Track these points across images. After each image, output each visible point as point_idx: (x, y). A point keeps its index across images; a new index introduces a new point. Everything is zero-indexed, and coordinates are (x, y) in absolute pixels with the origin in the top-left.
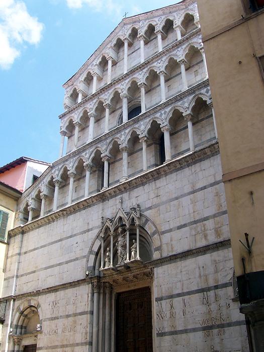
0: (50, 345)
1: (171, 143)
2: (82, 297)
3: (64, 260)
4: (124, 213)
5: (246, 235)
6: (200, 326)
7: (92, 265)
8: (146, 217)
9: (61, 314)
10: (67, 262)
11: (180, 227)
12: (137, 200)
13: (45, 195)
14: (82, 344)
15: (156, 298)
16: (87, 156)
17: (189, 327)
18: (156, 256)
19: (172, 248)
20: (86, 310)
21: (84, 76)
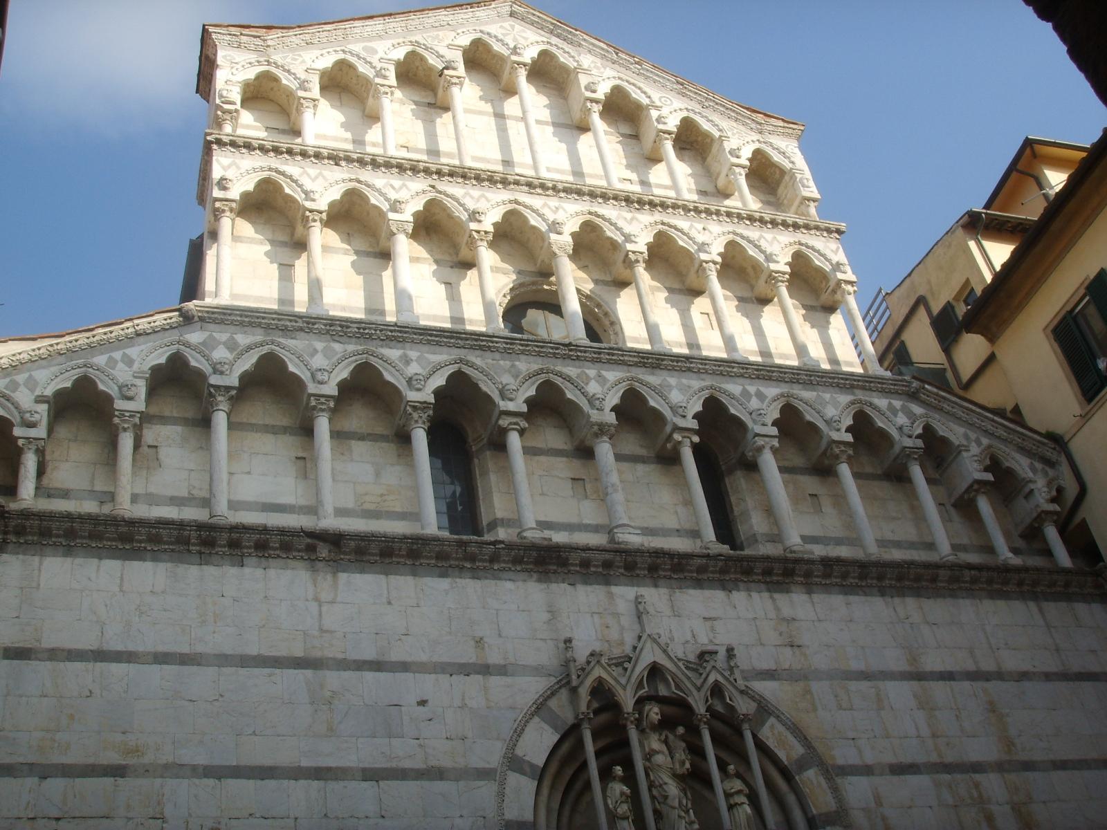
10: (372, 775)
11: (900, 769)
12: (713, 629)
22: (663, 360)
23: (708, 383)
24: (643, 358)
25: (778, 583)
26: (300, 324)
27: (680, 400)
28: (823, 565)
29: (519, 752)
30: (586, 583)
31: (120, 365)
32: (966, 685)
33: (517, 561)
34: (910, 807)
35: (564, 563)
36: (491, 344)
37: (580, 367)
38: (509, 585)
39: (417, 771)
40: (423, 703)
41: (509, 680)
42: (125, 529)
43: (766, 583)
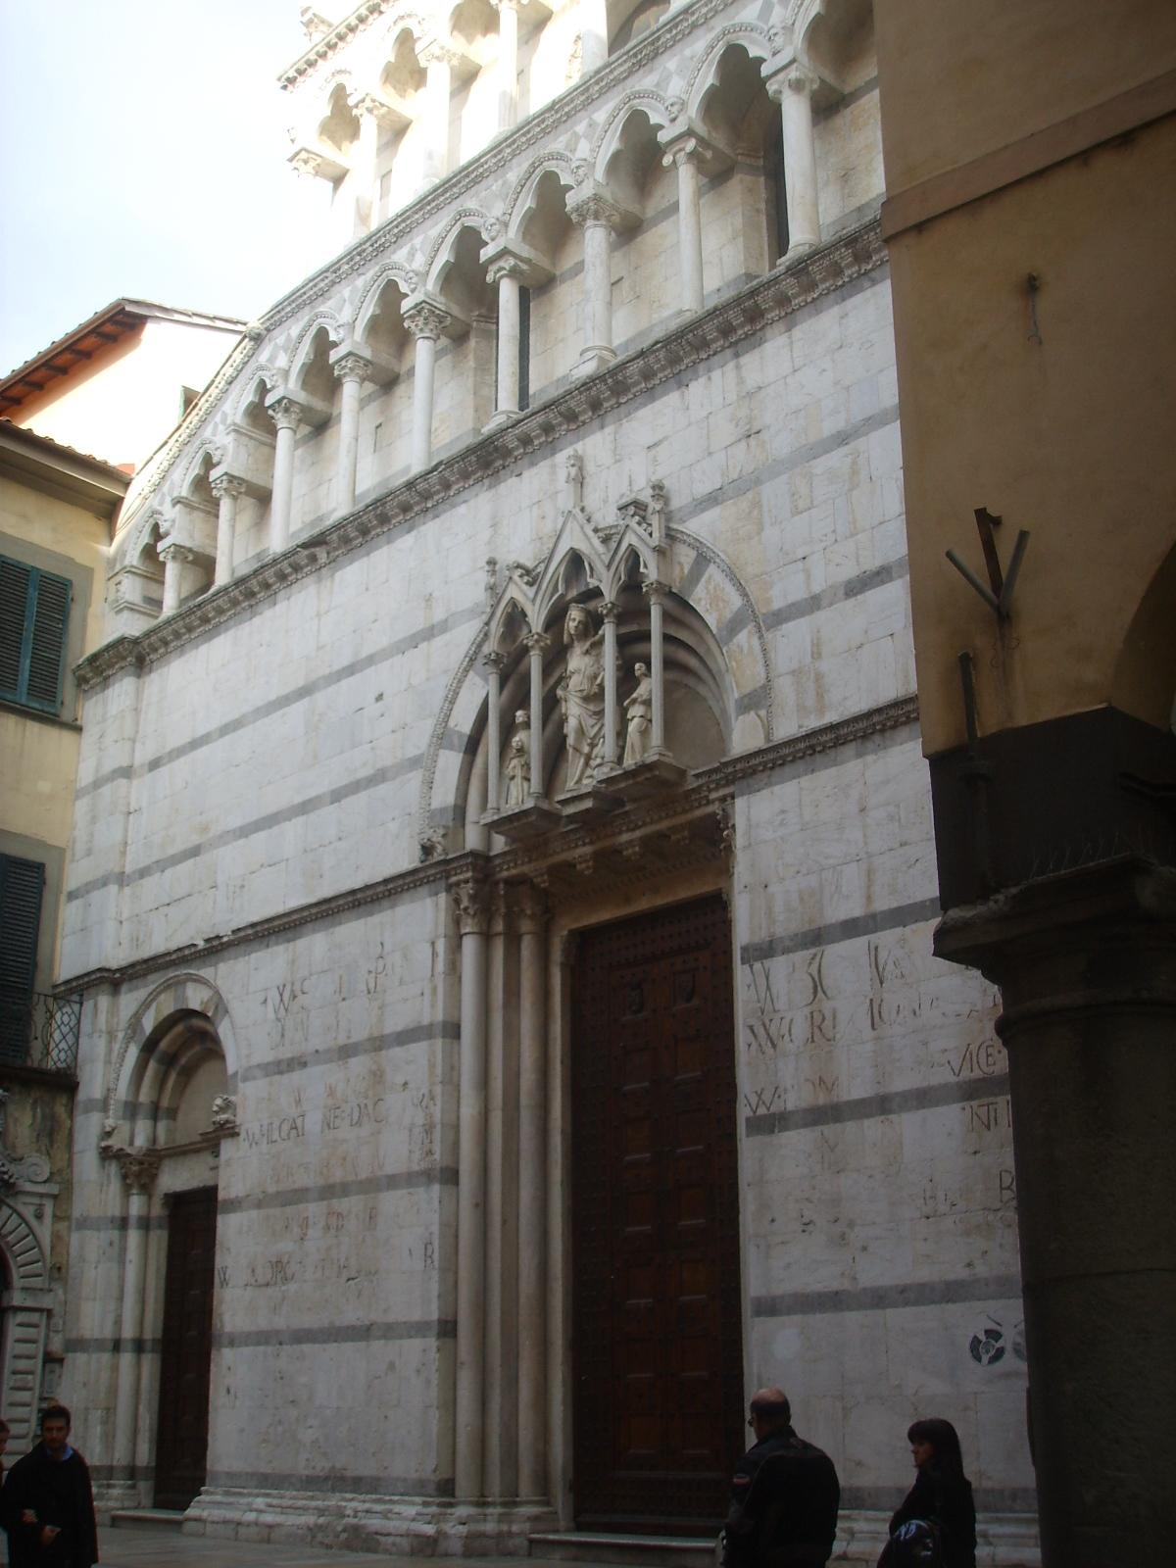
0: (272, 1189)
1: (816, 161)
2: (405, 956)
3: (323, 786)
4: (589, 529)
5: (987, 522)
6: (952, 1079)
8: (697, 545)
9: (317, 1042)
10: (337, 796)
12: (655, 460)
13: (232, 478)
14: (410, 1179)
15: (744, 949)
16: (419, 262)
17: (900, 1084)
18: (744, 737)
19: (820, 696)
20: (426, 1021)
22: (659, 38)
23: (718, 30)
24: (635, 55)
25: (747, 336)
26: (332, 276)
28: (792, 275)
30: (533, 464)
33: (465, 476)
34: (861, 646)
35: (506, 453)
36: (481, 170)
37: (567, 131)
38: (462, 509)
41: (446, 637)
42: (199, 613)
43: (732, 345)
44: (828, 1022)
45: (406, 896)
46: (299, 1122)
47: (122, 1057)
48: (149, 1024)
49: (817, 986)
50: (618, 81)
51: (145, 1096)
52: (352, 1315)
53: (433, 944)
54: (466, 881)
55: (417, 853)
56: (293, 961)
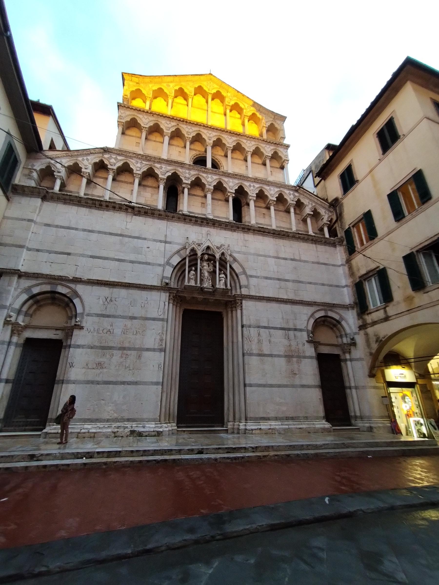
7: (170, 276)
9: (120, 313)
10: (132, 262)
21: (156, 87)
27: (231, 186)
29: (170, 261)
31: (85, 160)
32: (290, 262)
38: (176, 224)
39: (143, 262)
40: (148, 248)
44: (261, 341)
45: (157, 291)
46: (111, 331)
47: (18, 297)
48: (36, 290)
49: (259, 335)
50: (219, 174)
51: (25, 309)
52: (130, 378)
53: (164, 302)
54: (174, 293)
55: (164, 284)
56: (112, 293)
